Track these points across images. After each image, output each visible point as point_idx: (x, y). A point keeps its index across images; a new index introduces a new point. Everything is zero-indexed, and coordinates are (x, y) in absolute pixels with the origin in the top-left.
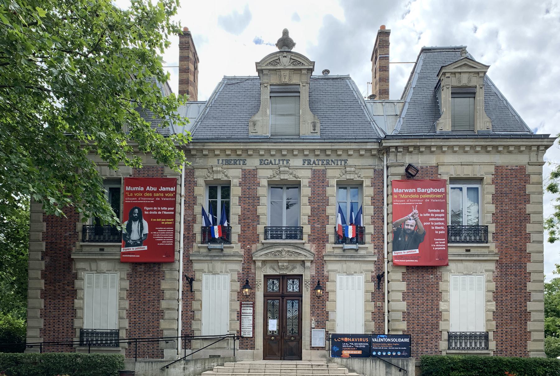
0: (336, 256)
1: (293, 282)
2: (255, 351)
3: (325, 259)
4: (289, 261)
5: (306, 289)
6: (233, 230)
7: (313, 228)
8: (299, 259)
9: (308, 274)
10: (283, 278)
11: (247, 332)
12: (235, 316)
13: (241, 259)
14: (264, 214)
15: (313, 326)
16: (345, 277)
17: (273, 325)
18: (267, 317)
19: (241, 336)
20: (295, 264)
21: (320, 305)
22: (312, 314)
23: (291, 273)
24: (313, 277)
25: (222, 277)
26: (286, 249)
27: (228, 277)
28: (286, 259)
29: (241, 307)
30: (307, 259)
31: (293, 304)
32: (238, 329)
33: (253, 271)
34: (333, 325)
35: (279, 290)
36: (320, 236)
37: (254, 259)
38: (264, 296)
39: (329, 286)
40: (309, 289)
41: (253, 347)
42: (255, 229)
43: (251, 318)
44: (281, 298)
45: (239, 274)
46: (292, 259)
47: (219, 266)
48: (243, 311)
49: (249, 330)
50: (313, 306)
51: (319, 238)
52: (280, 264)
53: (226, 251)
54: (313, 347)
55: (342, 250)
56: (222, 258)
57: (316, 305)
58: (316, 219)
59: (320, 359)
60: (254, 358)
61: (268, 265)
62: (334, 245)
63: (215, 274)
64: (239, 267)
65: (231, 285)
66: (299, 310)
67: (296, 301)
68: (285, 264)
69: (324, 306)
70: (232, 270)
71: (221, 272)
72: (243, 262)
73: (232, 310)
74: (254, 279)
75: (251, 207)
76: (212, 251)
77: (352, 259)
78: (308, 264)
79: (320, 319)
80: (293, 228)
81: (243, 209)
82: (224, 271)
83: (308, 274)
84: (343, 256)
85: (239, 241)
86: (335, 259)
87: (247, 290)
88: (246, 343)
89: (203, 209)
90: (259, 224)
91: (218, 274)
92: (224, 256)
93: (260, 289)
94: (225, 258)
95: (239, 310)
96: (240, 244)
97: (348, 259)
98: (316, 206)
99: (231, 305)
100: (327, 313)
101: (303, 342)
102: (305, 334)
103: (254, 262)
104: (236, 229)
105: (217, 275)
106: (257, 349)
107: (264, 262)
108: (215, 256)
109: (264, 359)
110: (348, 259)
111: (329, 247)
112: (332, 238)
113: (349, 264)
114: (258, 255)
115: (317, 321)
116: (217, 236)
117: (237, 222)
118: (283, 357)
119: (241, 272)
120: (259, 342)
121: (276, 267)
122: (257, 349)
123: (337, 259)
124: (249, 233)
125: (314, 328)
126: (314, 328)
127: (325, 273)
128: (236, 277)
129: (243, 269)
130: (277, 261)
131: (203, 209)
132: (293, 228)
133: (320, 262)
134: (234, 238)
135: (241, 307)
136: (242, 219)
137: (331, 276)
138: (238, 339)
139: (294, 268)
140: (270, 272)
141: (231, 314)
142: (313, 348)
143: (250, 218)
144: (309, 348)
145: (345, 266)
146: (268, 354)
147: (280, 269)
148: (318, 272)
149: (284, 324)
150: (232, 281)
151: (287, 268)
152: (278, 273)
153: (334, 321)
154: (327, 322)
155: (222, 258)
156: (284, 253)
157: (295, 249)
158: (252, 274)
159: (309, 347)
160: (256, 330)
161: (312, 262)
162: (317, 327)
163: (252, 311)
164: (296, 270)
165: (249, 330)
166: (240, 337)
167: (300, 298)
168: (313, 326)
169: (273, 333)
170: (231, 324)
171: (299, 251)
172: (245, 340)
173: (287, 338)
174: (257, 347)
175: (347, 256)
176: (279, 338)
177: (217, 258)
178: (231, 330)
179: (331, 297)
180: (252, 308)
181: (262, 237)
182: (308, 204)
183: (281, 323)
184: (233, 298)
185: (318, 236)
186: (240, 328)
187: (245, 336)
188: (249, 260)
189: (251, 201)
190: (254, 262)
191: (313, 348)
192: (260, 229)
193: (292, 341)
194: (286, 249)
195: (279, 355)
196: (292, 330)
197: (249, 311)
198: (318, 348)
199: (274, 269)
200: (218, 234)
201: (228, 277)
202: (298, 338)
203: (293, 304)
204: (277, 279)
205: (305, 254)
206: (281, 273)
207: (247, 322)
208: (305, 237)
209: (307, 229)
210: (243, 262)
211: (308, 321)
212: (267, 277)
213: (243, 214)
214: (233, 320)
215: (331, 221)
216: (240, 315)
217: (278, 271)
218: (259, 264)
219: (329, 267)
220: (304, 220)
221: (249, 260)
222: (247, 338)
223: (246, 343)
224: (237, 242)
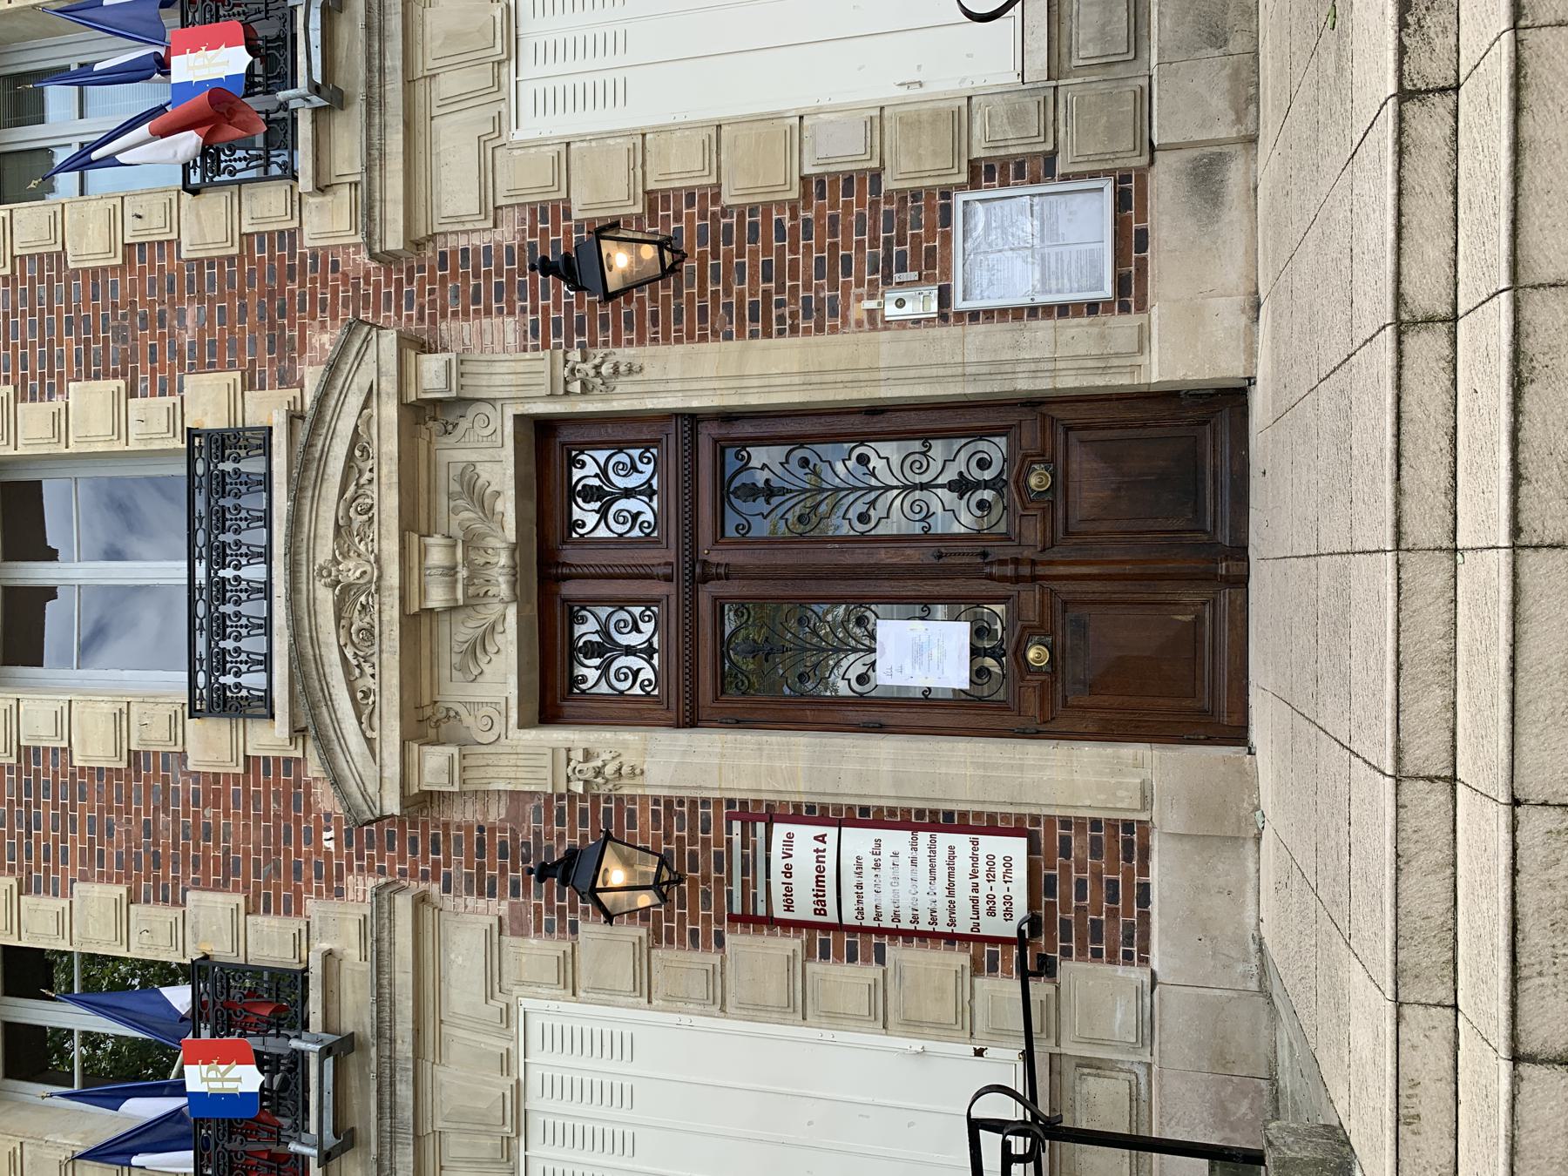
0: (373, 158)
1: (590, 494)
2: (1166, 820)
3: (394, 240)
4: (413, 522)
5: (622, 385)
6: (222, 950)
7: (207, 359)
8: (391, 446)
9: (513, 370)
10: (553, 574)
11: (990, 880)
12: (846, 979)
13: (403, 904)
14: (121, 717)
15: (921, 303)
16: (533, 74)
17: (924, 651)
18: (861, 701)
19: (1021, 941)
20: (446, 482)
21: (753, 256)
22: (821, 316)
23: (507, 506)
24: (538, 335)
25: (543, 1064)
26: (325, 549)
27: (545, 1011)
28: (391, 547)
29: (770, 922)
30: (389, 386)
31: (752, 492)
32: (960, 958)
33: (497, 813)
34: (912, 123)
35: (647, 602)
36: (253, 295)
37: (392, 806)
38: (690, 719)
39: (601, 192)
40: (624, 354)
41: (1127, 840)
42: (212, 786)
43: (858, 841)
44: (706, 593)
45: (520, 931)
46: (391, 502)
47: (460, 1084)
48: (804, 909)
49: (963, 864)
50: (762, 320)
51: (267, 298)
52: (437, 597)
53: (356, 1014)
54: (1122, 284)
55: (339, 119)
56: (404, 1048)
57: (748, 290)
58: (146, 338)
59: (1233, 213)
60: (1228, 831)
61: (455, 692)
62: (305, 183)
63: (520, 1119)
64: (469, 924)
65: (604, 993)
66: (798, 441)
67: (732, 464)
68: (437, 556)
69: (756, 221)
70: (494, 981)
71: (505, 1063)
72: (435, 889)
73: (798, 1006)
74: (556, 806)
75: (85, 810)
76: (354, 1121)
77: (395, 23)
78: (432, 374)
79: (862, 249)
80: (200, 505)
81: (95, 866)
82: (500, 1045)
83: (513, 370)
84: (375, 103)
85: (293, 907)
86: (395, 165)
87: (617, 875)
88: (1083, 899)
89: (98, 1154)
90: (183, 756)
91: (519, 1089)
92: (383, 1031)
93: (628, 759)
94: (404, 1028)
95: (794, 943)
96: (311, 905)
97: (394, 61)
98: (69, 345)
99: (755, 1010)
100: (814, 186)
101: (1068, 382)
102: (997, 368)
103: (420, 802)
104: (213, 924)
105: (534, 1102)
106: (1146, 800)
107: (425, 722)
108: (387, 1107)
109: (1237, 735)
110: (394, 61)
111: (327, 224)
112: (266, 207)
113: (431, 54)
114: (369, 772)
115: (886, 271)
116: (249, 1079)
117: (170, 913)
118: (1223, 565)
119: (502, 907)
120: (1076, 776)
121: (465, 630)
122: (1146, 800)
123: (395, 142)
124: (242, 834)
125: (944, 296)
126: (944, 296)
127: (507, 234)
128: (535, 952)
129: (487, 889)
130: (415, 622)
131: (98, 1154)
132: (200, 505)
133: (423, 280)
134: (269, 942)
135: (770, 922)
136: (153, 878)
137: (525, 179)
138: (1046, 968)
139: (472, 490)
140: (501, 676)
141: (834, 1018)
142: (1130, 288)
143: (142, 821)
144: (1133, 319)
145: (449, 84)
146: (1194, 695)
147: (474, 602)
148: (504, 297)
149: (914, 555)
150: (568, 979)
151: (472, 541)
152: (512, 612)
153: (877, 121)
154: (889, 183)
155: (404, 1048)
156: (351, 570)
157: (321, 478)
158: (515, 816)
159: (1122, 326)
160: (963, 796)
161: (416, 344)
162: (932, 263)
163: (804, 834)
164: (485, 473)
165: (963, 864)
166: (1032, 953)
167: (707, 433)
168: (921, 303)
169: (994, 654)
170: (913, 1026)
171: (339, 450)
172: (1064, 906)
173: (1033, 533)
174: (1124, 805)
175: (375, 69)
176: (1031, 597)
177: (404, 1091)
178: (964, 1023)
179: (679, 168)
180: (780, 831)
181: (270, 738)
182: (58, 402)
183: (909, 588)
184: (699, 991)
185: (253, 316)
186: (951, 939)
187: (1021, 908)
188: (416, 836)
189: (47, 812)
190: (420, 802)
191: (1130, 288)
192: (211, 746)
193: (1061, 483)
194: (325, 549)
195: (1190, 595)
196: (962, 486)
197: (798, 852)
198: (1131, 242)
199: (478, 647)
200: (238, 1070)
201: (545, 1011)
202: (1030, 437)
203: (752, 492)
204: (574, 619)
205: (354, 401)
206: (503, 589)
207: (896, 876)
208: (266, 409)
209: (209, 400)
210: (435, 889)
211: (887, 348)
212: (551, 698)
213: (124, 870)
214: (879, 991)
215: (154, 228)
216: (840, 938)
217: (493, 611)
218: (434, 767)
219: (456, 197)
220: (152, 425)
221: (416, 836)
222: (1038, 885)
223: (1083, 899)
224: (297, 924)
